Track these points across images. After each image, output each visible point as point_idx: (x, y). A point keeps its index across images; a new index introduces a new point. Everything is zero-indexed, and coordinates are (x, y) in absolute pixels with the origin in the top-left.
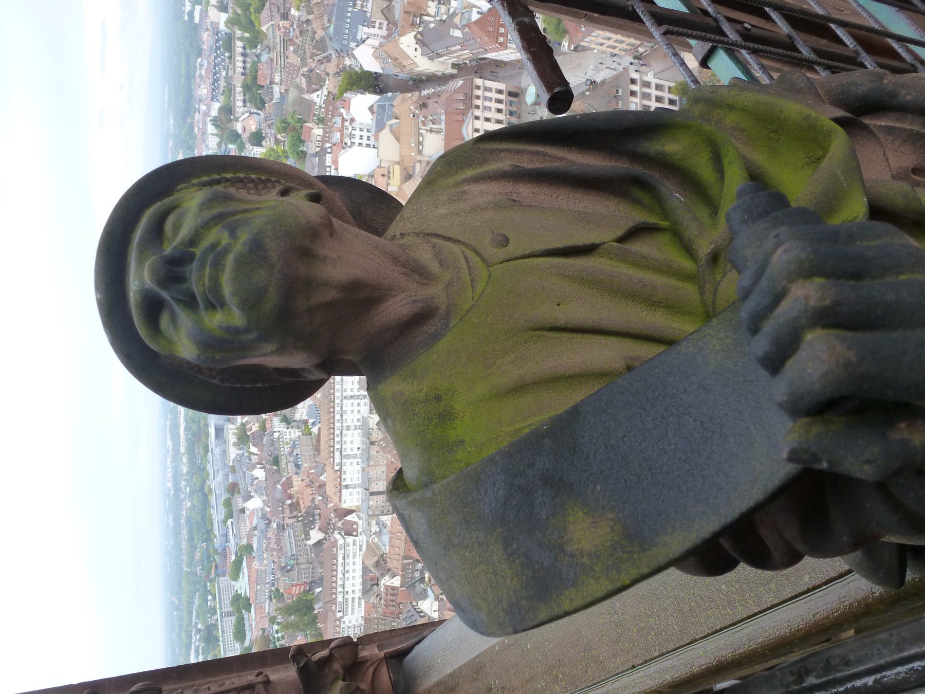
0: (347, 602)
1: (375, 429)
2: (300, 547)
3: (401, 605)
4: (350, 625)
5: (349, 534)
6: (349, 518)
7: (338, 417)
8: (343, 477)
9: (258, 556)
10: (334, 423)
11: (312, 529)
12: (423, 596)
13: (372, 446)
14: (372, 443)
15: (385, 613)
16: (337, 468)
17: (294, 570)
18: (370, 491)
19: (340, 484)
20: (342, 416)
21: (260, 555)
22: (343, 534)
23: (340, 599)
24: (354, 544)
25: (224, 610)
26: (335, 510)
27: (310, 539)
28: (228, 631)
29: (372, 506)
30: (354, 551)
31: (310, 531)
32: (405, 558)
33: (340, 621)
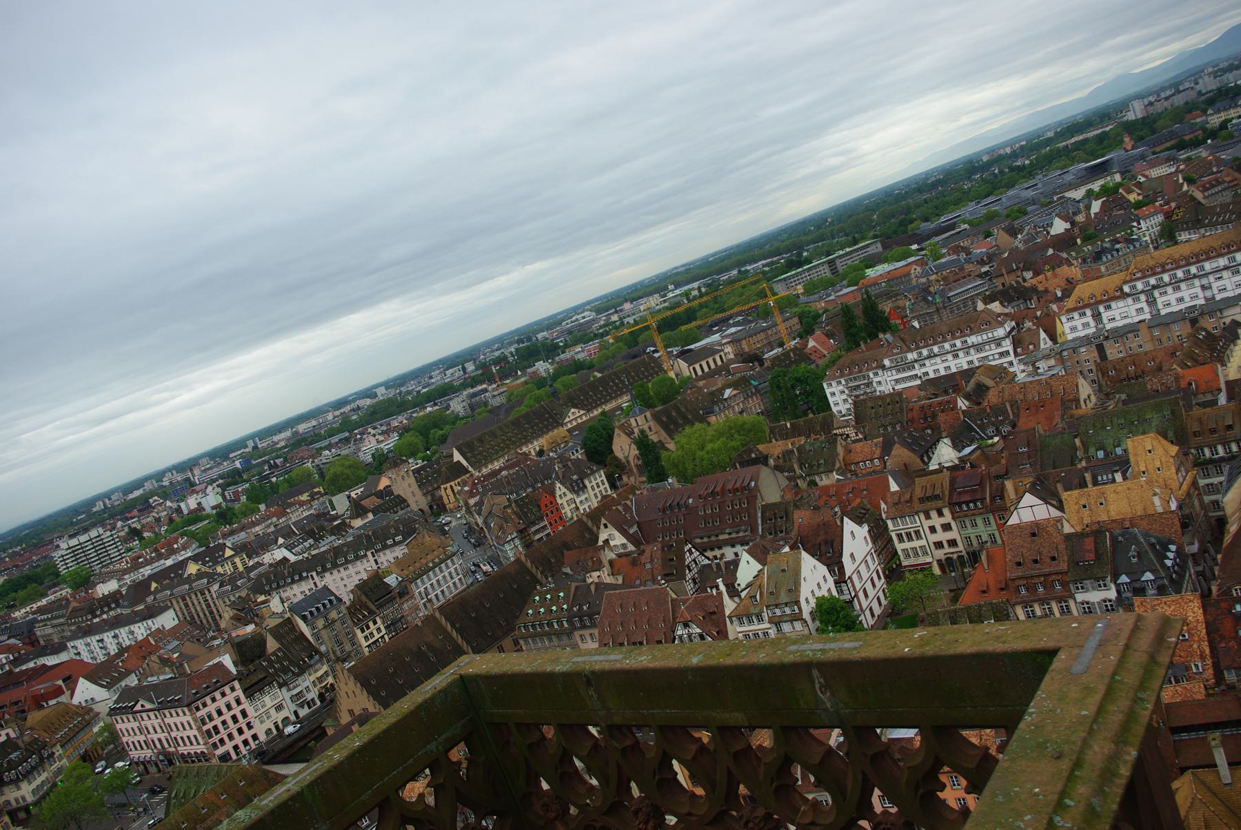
0: (909, 369)
1: (1223, 320)
2: (965, 307)
3: (929, 431)
4: (875, 385)
5: (1016, 343)
6: (1043, 335)
7: (1222, 262)
8: (1113, 304)
9: (930, 268)
10: (1208, 259)
11: (1001, 303)
12: (957, 445)
13: (1188, 324)
14: (1194, 322)
15: (912, 410)
16: (1126, 289)
17: (929, 308)
18: (1105, 343)
19: (1101, 302)
20: (1226, 268)
21: (932, 271)
22: (1013, 333)
23: (911, 356)
24: (1002, 355)
25: (838, 262)
26: (1047, 315)
27: (986, 304)
28: (812, 276)
29: (1079, 353)
30: (991, 358)
31: (997, 303)
32: (1014, 403)
33: (877, 368)
